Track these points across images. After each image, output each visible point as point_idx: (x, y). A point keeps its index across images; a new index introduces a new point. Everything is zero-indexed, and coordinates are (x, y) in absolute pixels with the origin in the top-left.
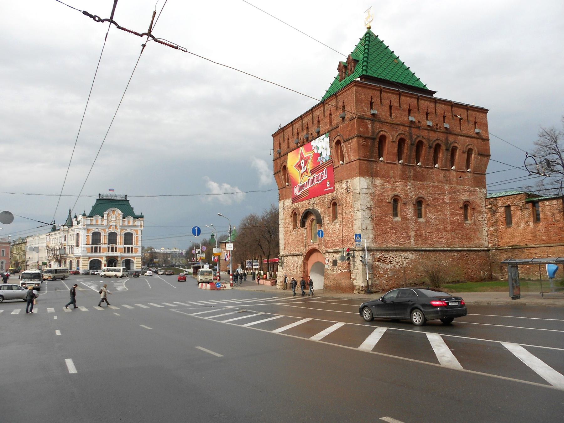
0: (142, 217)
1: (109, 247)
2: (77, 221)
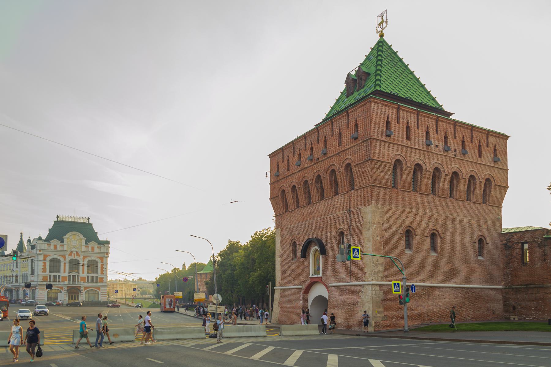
0: (108, 242)
1: (69, 276)
2: (32, 246)
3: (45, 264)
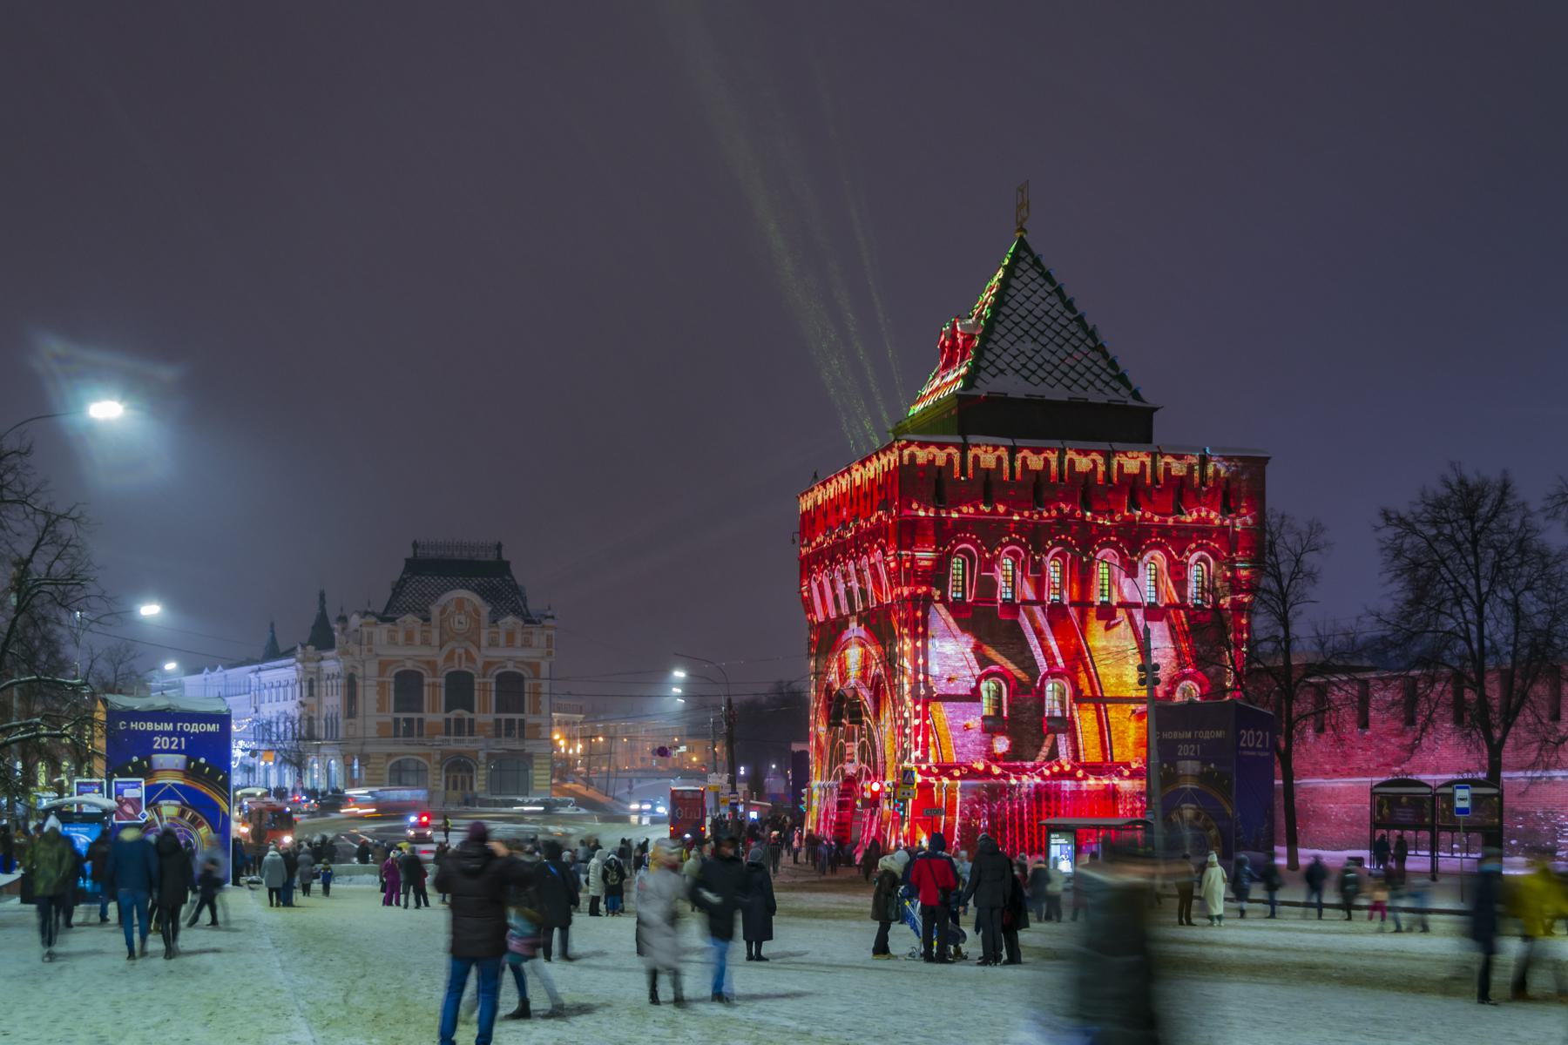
1: (448, 720)
3: (382, 685)
